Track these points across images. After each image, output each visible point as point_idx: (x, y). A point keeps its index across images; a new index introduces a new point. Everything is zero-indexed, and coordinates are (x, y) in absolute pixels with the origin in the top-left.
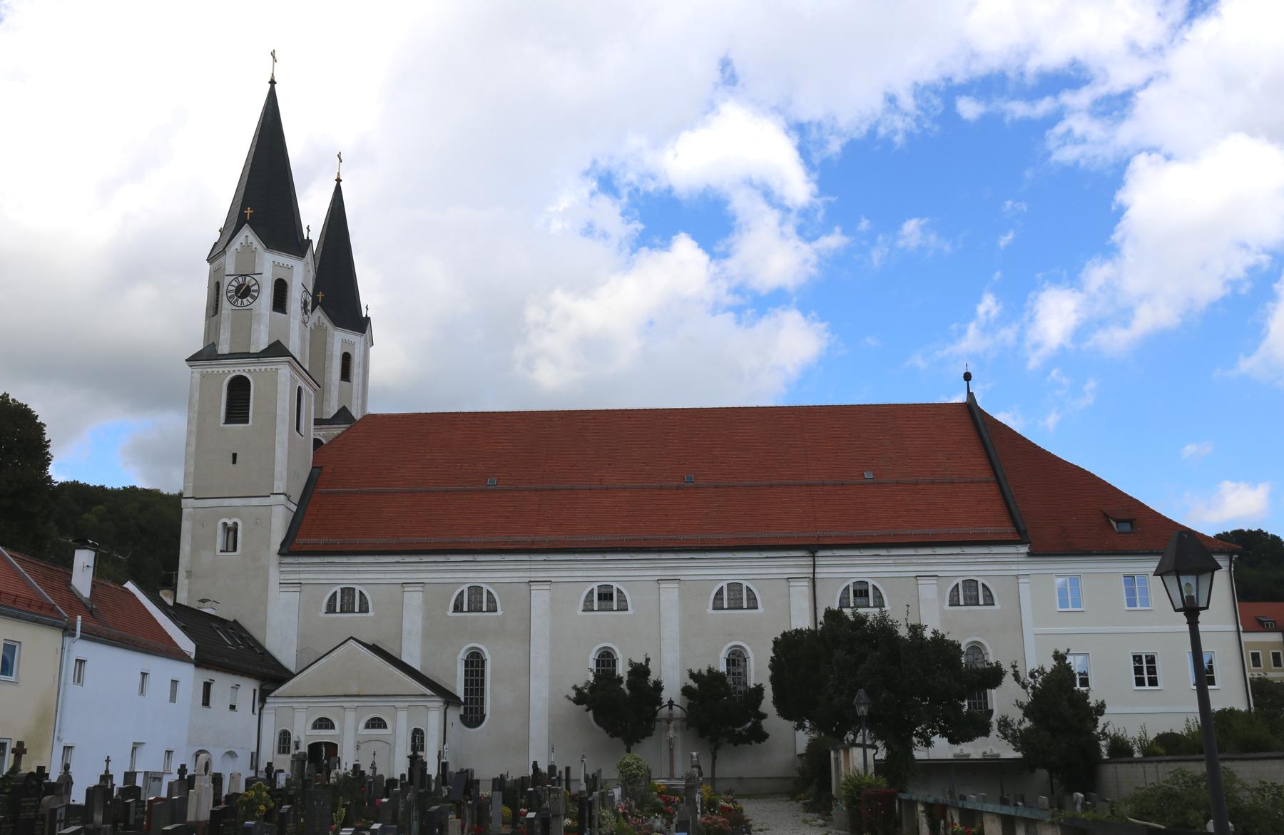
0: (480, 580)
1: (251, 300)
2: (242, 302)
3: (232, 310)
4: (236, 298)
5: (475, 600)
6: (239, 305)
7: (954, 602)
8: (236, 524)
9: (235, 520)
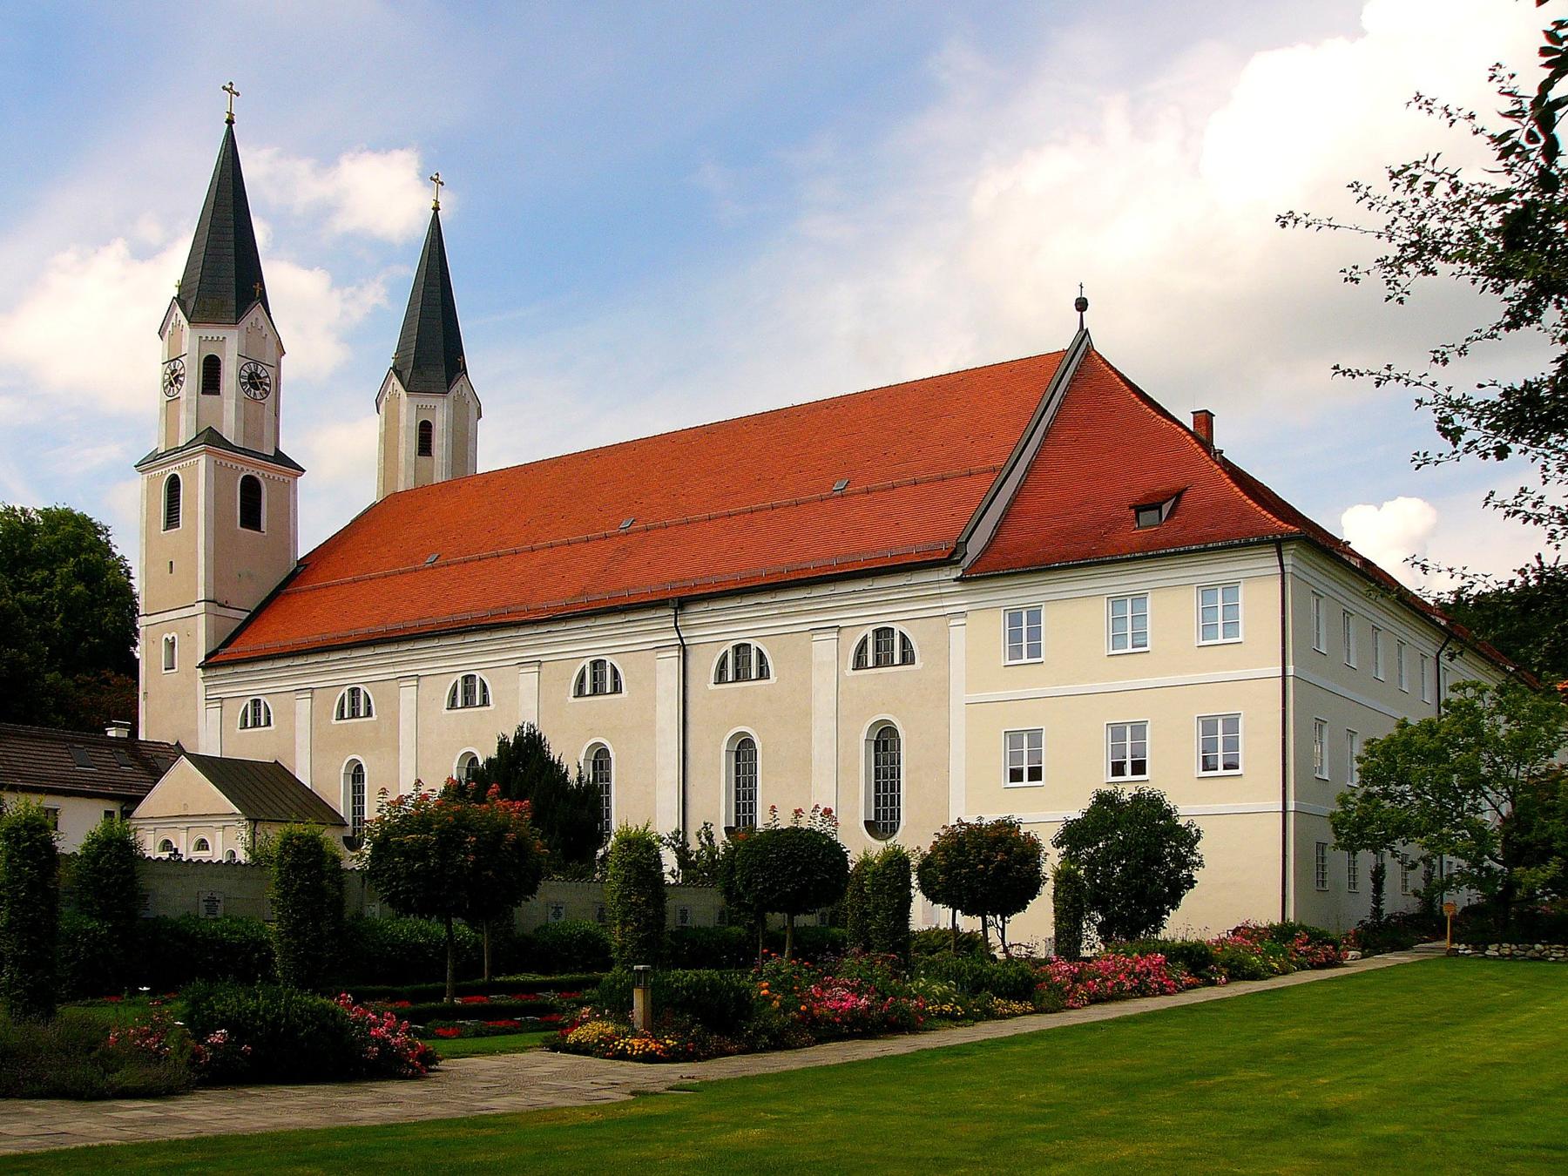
0: (357, 681)
5: (355, 704)
7: (859, 663)
8: (173, 638)
9: (174, 634)
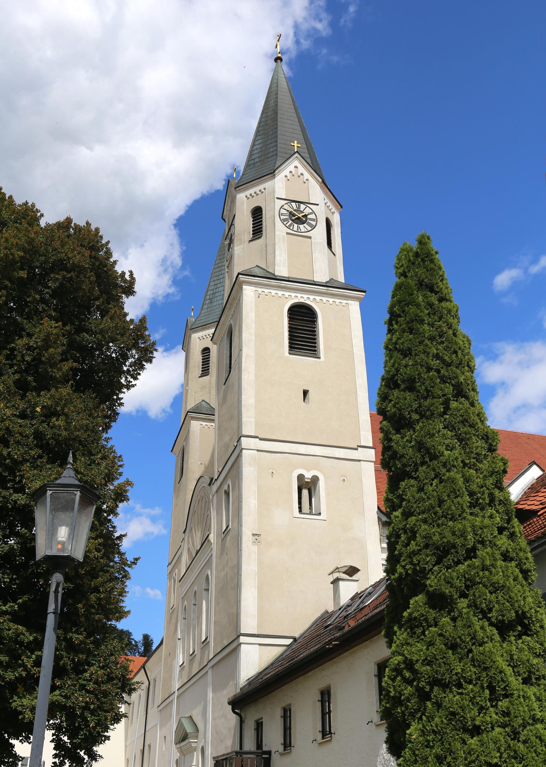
1: (309, 228)
2: (298, 227)
3: (287, 233)
4: (291, 222)
6: (295, 229)
8: (315, 479)
9: (316, 473)
